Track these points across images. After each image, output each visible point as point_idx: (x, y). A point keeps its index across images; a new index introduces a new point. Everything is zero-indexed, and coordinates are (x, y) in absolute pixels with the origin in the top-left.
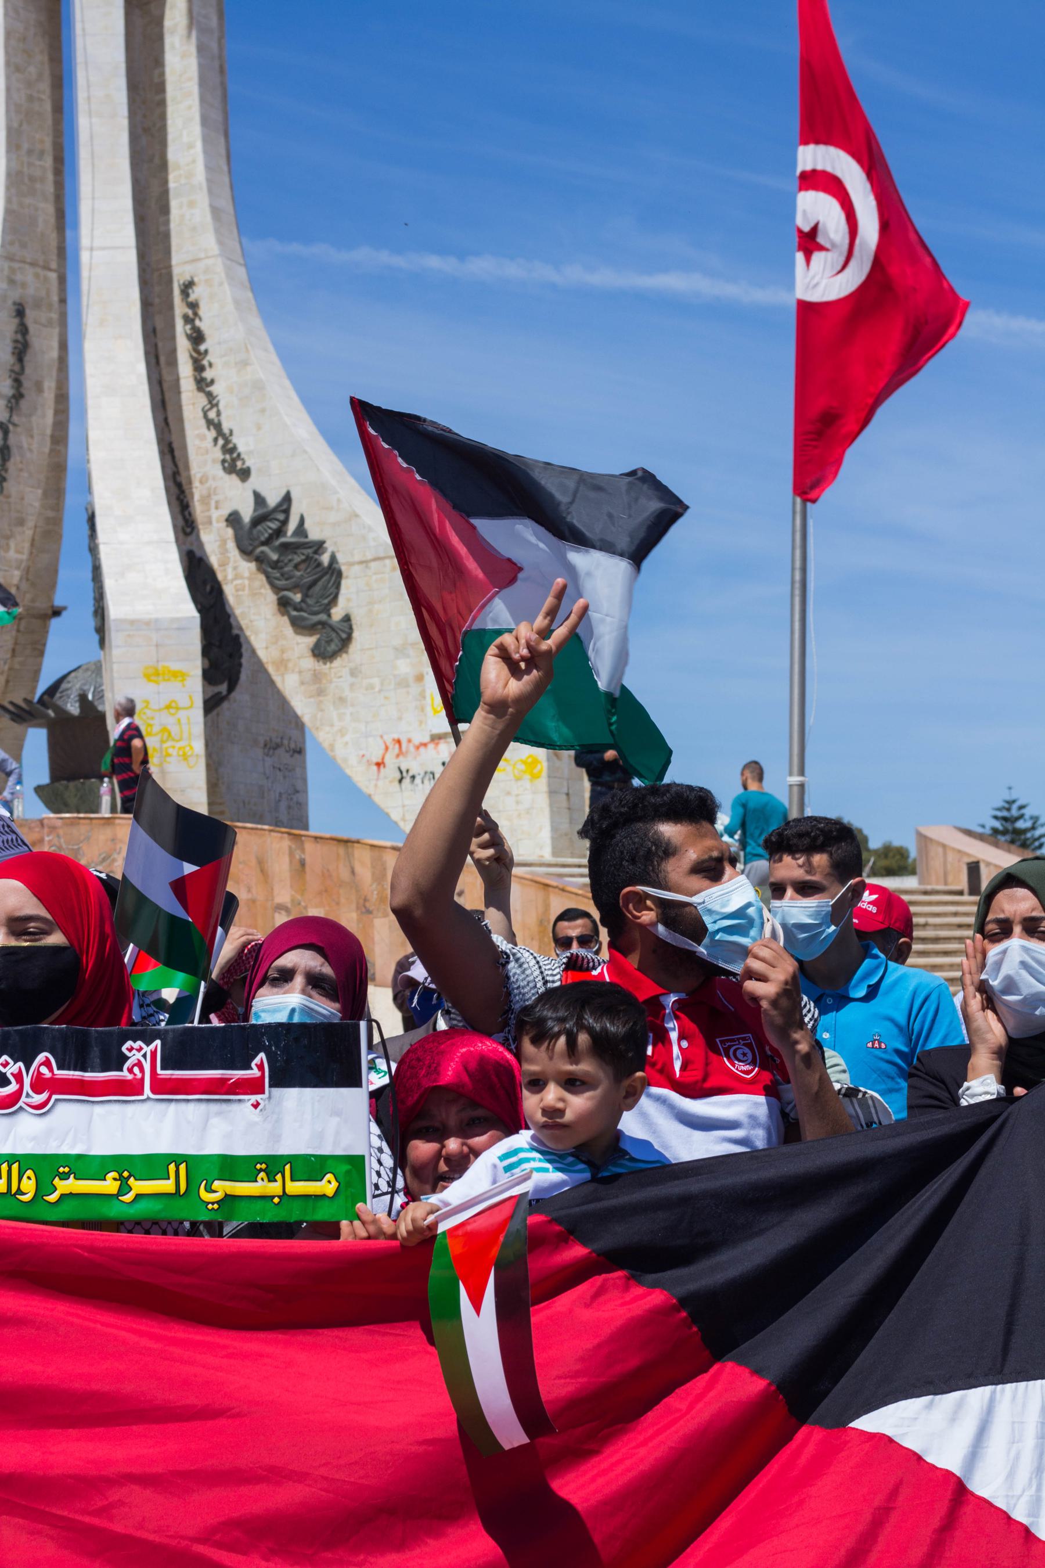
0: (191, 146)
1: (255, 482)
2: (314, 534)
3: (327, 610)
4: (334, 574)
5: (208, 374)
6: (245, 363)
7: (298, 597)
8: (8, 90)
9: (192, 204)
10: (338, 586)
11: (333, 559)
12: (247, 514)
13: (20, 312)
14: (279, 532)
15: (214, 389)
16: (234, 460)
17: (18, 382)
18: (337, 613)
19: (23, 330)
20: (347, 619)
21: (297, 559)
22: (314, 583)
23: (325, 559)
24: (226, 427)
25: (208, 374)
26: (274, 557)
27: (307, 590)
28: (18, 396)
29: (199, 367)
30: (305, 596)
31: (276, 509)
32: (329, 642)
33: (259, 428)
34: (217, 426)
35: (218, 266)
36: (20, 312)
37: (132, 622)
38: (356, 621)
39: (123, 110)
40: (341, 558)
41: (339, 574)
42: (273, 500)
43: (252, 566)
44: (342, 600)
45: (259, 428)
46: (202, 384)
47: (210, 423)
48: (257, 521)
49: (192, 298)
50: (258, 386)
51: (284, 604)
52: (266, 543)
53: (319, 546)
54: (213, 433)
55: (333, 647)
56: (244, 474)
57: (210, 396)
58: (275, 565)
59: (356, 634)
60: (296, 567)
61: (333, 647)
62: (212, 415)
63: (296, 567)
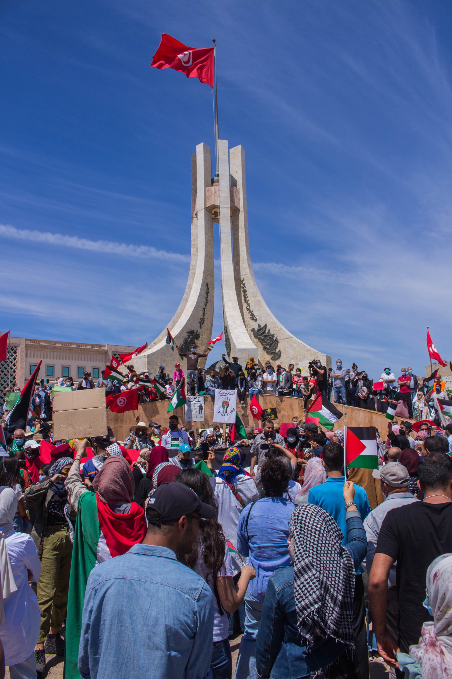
0: (243, 251)
1: (258, 322)
2: (272, 333)
3: (275, 349)
4: (277, 342)
5: (247, 299)
6: (256, 296)
7: (268, 347)
8: (205, 238)
9: (243, 263)
10: (278, 344)
11: (276, 338)
12: (256, 329)
13: (207, 285)
14: (264, 333)
15: (249, 302)
16: (253, 317)
17: (207, 300)
18: (277, 350)
19: (208, 289)
20: (280, 351)
21: (268, 338)
22: (272, 344)
23: (275, 339)
24: (251, 310)
25: (247, 299)
26: (263, 338)
27: (270, 345)
28: (207, 303)
29: (245, 298)
30: (270, 346)
31: (263, 328)
32: (275, 357)
33: (259, 310)
34: (250, 310)
35: (250, 276)
36: (207, 285)
37: (243, 349)
38: (282, 352)
39: (230, 243)
40: (278, 338)
41: (278, 342)
42: (262, 326)
43: (258, 340)
44: (278, 347)
45: (259, 310)
46: (246, 301)
47: (248, 309)
48: (258, 330)
49: (244, 283)
50: (259, 301)
51: (265, 348)
52: (261, 335)
53: (273, 336)
54: (248, 311)
55: (276, 357)
56: (256, 320)
57: (248, 304)
58: (263, 340)
59: (282, 355)
60: (268, 340)
61: (276, 357)
62: (248, 307)
63: (268, 340)
